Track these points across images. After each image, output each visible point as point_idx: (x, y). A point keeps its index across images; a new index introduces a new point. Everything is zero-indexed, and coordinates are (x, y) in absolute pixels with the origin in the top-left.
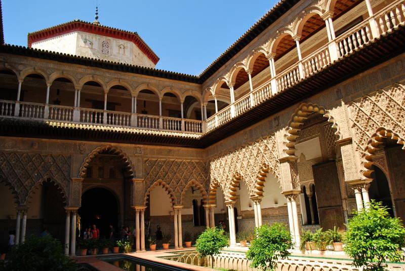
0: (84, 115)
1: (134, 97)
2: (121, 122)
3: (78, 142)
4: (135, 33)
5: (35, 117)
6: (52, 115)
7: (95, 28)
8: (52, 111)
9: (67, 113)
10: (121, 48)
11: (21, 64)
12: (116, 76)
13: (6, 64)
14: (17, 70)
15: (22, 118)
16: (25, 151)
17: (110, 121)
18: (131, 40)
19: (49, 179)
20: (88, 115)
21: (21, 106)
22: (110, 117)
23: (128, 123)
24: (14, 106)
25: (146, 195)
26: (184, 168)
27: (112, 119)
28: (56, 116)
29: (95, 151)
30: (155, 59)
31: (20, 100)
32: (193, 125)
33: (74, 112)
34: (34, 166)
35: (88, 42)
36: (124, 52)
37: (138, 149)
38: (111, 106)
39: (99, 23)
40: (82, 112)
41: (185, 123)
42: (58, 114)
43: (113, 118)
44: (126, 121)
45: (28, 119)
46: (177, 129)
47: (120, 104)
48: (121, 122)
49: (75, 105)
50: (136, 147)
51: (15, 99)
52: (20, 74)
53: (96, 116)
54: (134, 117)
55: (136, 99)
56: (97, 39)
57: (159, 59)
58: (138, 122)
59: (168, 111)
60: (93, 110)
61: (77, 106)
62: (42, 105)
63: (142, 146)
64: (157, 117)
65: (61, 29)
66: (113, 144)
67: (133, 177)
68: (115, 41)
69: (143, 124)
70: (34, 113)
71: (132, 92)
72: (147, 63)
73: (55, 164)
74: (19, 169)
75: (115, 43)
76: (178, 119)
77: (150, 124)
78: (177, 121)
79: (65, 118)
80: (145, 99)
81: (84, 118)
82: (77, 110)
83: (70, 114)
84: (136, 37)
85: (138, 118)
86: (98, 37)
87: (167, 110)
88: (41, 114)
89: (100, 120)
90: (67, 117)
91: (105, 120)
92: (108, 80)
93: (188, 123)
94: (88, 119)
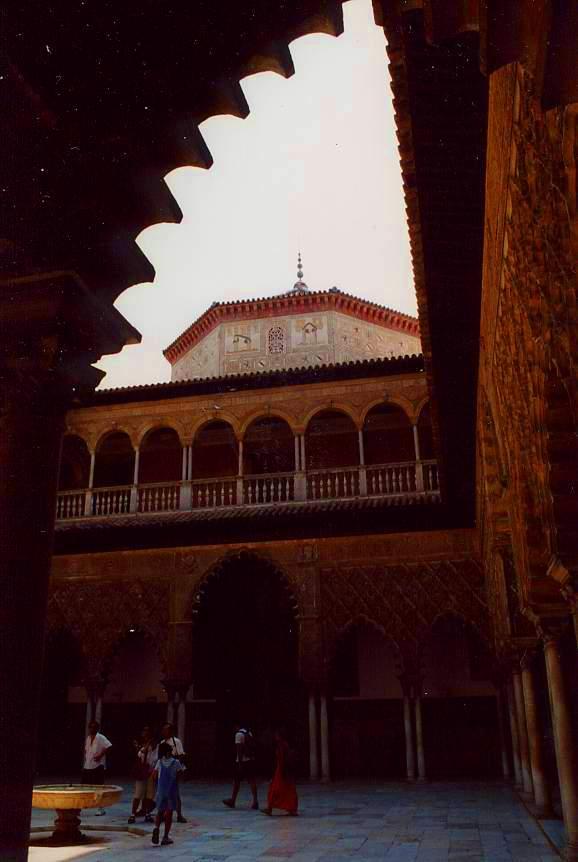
1: (299, 437)
6: (143, 504)
8: (144, 497)
10: (307, 331)
11: (92, 421)
12: (258, 401)
15: (98, 518)
27: (253, 493)
28: (150, 504)
31: (95, 486)
37: (306, 548)
38: (254, 465)
39: (303, 284)
40: (195, 488)
43: (257, 488)
44: (284, 490)
46: (405, 489)
50: (299, 546)
54: (300, 481)
56: (257, 331)
58: (309, 487)
62: (126, 488)
66: (250, 545)
70: (114, 505)
71: (293, 425)
85: (309, 480)
86: (260, 322)
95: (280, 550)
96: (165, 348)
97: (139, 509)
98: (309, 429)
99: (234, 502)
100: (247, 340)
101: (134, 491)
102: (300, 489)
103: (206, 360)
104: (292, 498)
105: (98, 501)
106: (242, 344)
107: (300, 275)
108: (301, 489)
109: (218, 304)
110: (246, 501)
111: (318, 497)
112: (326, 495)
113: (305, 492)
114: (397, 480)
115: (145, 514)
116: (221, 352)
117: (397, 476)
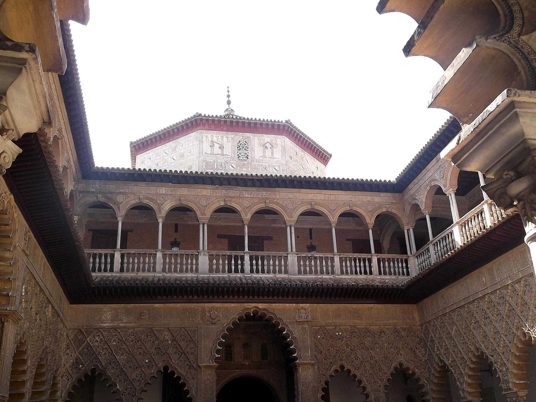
0: (215, 261)
2: (271, 268)
4: (287, 122)
5: (144, 270)
6: (167, 266)
7: (225, 122)
8: (168, 260)
9: (189, 261)
10: (266, 147)
11: (121, 193)
13: (100, 196)
14: (115, 204)
15: (124, 275)
16: (131, 325)
17: (255, 267)
18: (281, 134)
19: (166, 368)
20: (221, 262)
21: (122, 256)
22: (254, 262)
23: (283, 268)
24: (112, 256)
25: (320, 389)
26: (383, 339)
27: (257, 265)
28: (173, 266)
29: (235, 316)
30: (323, 157)
32: (392, 264)
33: (200, 258)
34: (143, 348)
35: (217, 146)
36: (272, 153)
37: (302, 311)
38: (257, 243)
41: (379, 260)
42: (176, 263)
45: (133, 275)
46: (366, 273)
47: (271, 238)
48: (271, 268)
49: (201, 248)
51: (115, 247)
52: (119, 208)
53: (233, 262)
54: (292, 259)
55: (293, 228)
57: (331, 156)
59: (351, 242)
60: (228, 253)
61: (203, 249)
62: (152, 251)
63: (308, 305)
64: (329, 255)
65: (176, 130)
66: (261, 306)
67: (296, 358)
68: (256, 138)
70: (141, 266)
71: (286, 218)
73: (175, 342)
74: (122, 354)
75: (256, 141)
77: (319, 268)
78: (364, 260)
79: (187, 268)
81: (215, 267)
82: (204, 255)
83: (194, 262)
84: (289, 127)
85: (299, 259)
86: (231, 135)
87: (348, 240)
89: (240, 267)
90: (189, 267)
91: (247, 267)
92: (247, 203)
94: (221, 267)
95: (281, 310)
96: (134, 139)
97: (164, 270)
99: (243, 271)
100: (221, 147)
101: (159, 255)
102: (293, 264)
103: (182, 156)
107: (229, 103)
108: (292, 266)
109: (200, 115)
110: (252, 271)
111: (305, 273)
112: (311, 273)
113: (297, 268)
116: (201, 152)
117: (360, 263)
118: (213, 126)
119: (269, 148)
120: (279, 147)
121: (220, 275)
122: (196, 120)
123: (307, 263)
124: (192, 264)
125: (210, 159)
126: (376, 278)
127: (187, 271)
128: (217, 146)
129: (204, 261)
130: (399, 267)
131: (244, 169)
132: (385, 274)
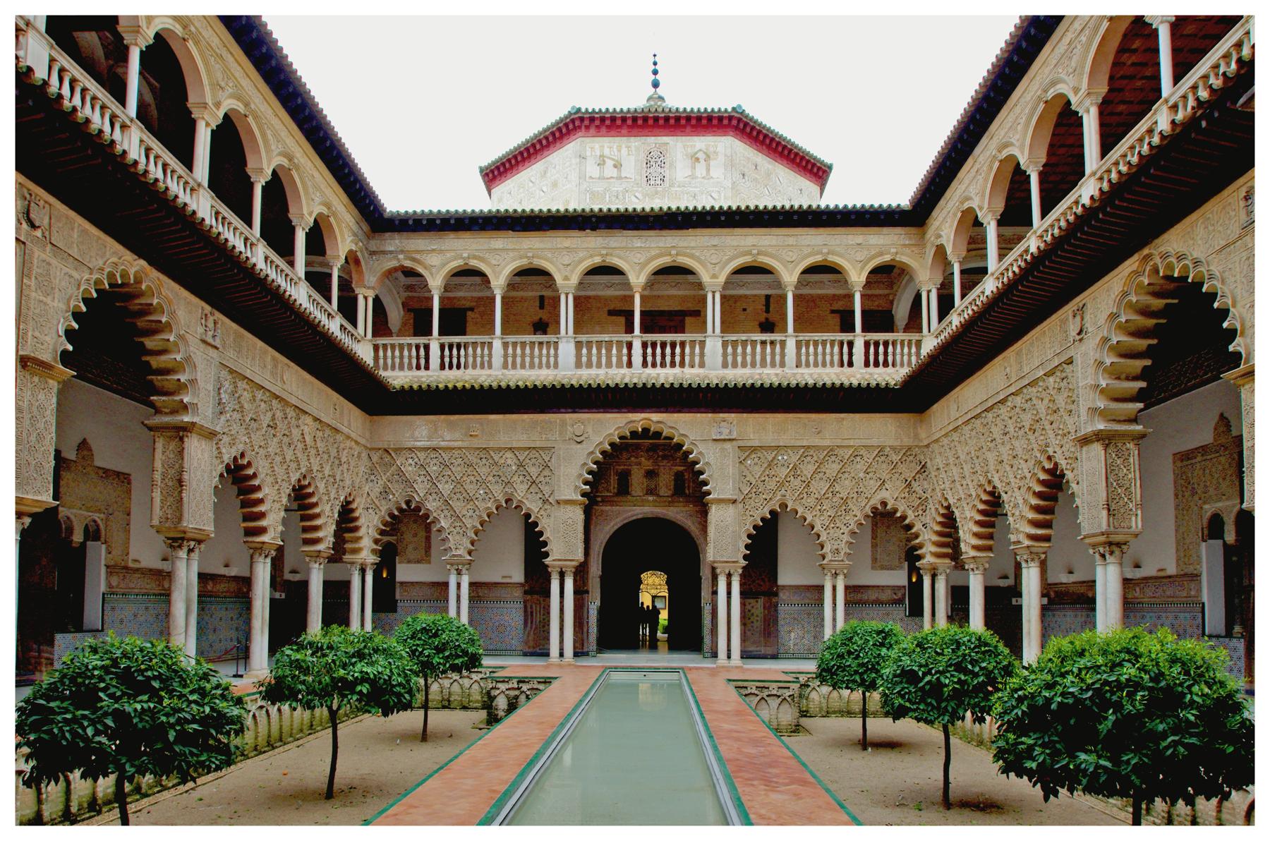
0: (584, 351)
2: (678, 359)
3: (569, 417)
6: (510, 360)
9: (544, 351)
10: (697, 159)
12: (661, 245)
17: (649, 359)
20: (594, 351)
21: (442, 347)
22: (649, 350)
24: (427, 347)
27: (654, 355)
32: (890, 349)
33: (561, 346)
35: (609, 163)
36: (708, 170)
39: (661, 98)
40: (579, 345)
41: (867, 344)
43: (659, 350)
48: (678, 359)
53: (614, 351)
54: (714, 345)
57: (830, 167)
58: (725, 355)
62: (486, 339)
63: (733, 415)
66: (655, 417)
68: (679, 144)
69: (739, 359)
71: (705, 278)
72: (791, 191)
75: (678, 146)
76: (846, 337)
77: (758, 358)
78: (841, 344)
80: (769, 292)
81: (584, 359)
83: (552, 351)
84: (739, 120)
85: (725, 344)
88: (486, 358)
90: (544, 360)
93: (877, 344)
94: (594, 359)
95: (687, 428)
97: (505, 366)
98: (727, 284)
99: (630, 364)
100: (618, 166)
101: (497, 345)
103: (555, 185)
104: (702, 365)
105: (447, 352)
106: (610, 171)
107: (656, 85)
109: (579, 110)
110: (645, 364)
113: (720, 359)
114: (832, 354)
115: (512, 372)
116: (582, 176)
118: (604, 130)
119: (702, 161)
120: (721, 158)
121: (593, 371)
122: (573, 121)
123: (740, 350)
124: (548, 355)
125: (599, 187)
126: (858, 375)
127: (540, 367)
128: (609, 163)
129: (567, 349)
130: (902, 355)
131: (657, 201)
132: (876, 364)
